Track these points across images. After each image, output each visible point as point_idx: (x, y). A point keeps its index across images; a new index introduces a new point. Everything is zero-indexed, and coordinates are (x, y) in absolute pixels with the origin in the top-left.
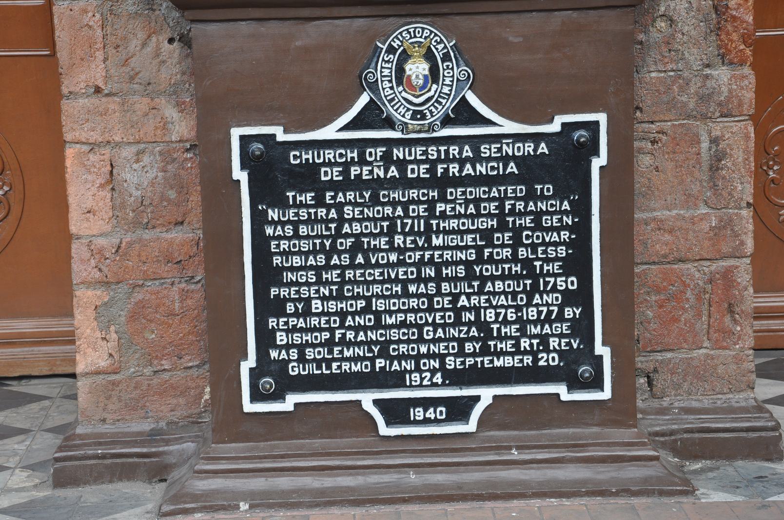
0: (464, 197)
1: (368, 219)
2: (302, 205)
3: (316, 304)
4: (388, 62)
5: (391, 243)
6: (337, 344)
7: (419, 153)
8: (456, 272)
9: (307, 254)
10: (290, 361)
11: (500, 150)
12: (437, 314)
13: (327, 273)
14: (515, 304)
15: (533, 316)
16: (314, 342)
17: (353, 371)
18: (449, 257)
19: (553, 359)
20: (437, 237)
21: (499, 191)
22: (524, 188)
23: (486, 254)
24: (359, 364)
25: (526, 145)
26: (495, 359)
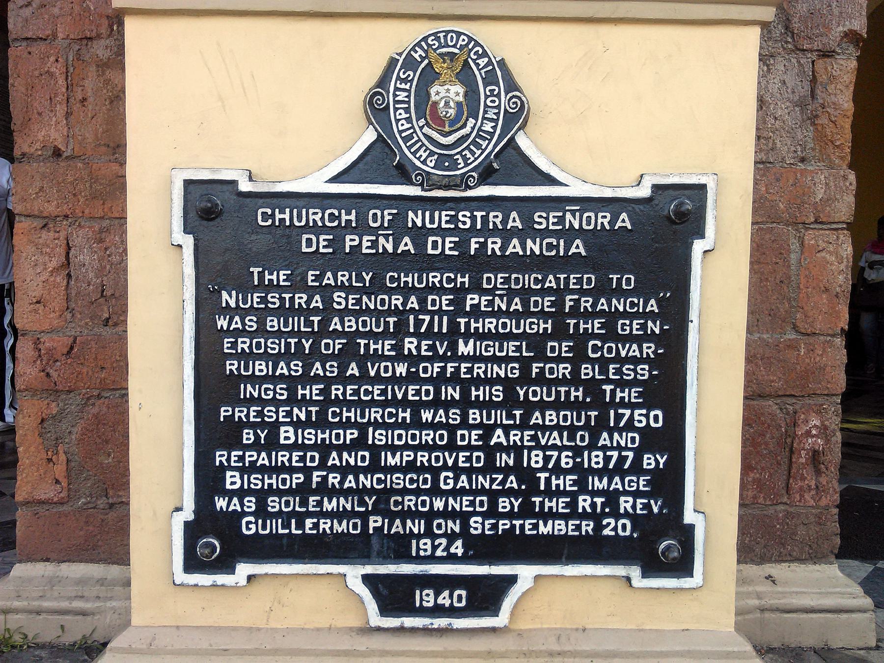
0: (507, 287)
1: (368, 311)
2: (272, 287)
3: (286, 432)
4: (405, 81)
5: (398, 347)
6: (314, 492)
7: (444, 219)
8: (491, 394)
9: (276, 359)
10: (244, 514)
11: (561, 220)
12: (461, 454)
13: (304, 388)
14: (573, 444)
15: (597, 463)
16: (281, 487)
17: (335, 532)
18: (481, 371)
19: (624, 527)
20: (466, 344)
21: (557, 280)
22: (593, 277)
23: (535, 371)
24: (345, 522)
25: (600, 215)
26: (541, 522)
